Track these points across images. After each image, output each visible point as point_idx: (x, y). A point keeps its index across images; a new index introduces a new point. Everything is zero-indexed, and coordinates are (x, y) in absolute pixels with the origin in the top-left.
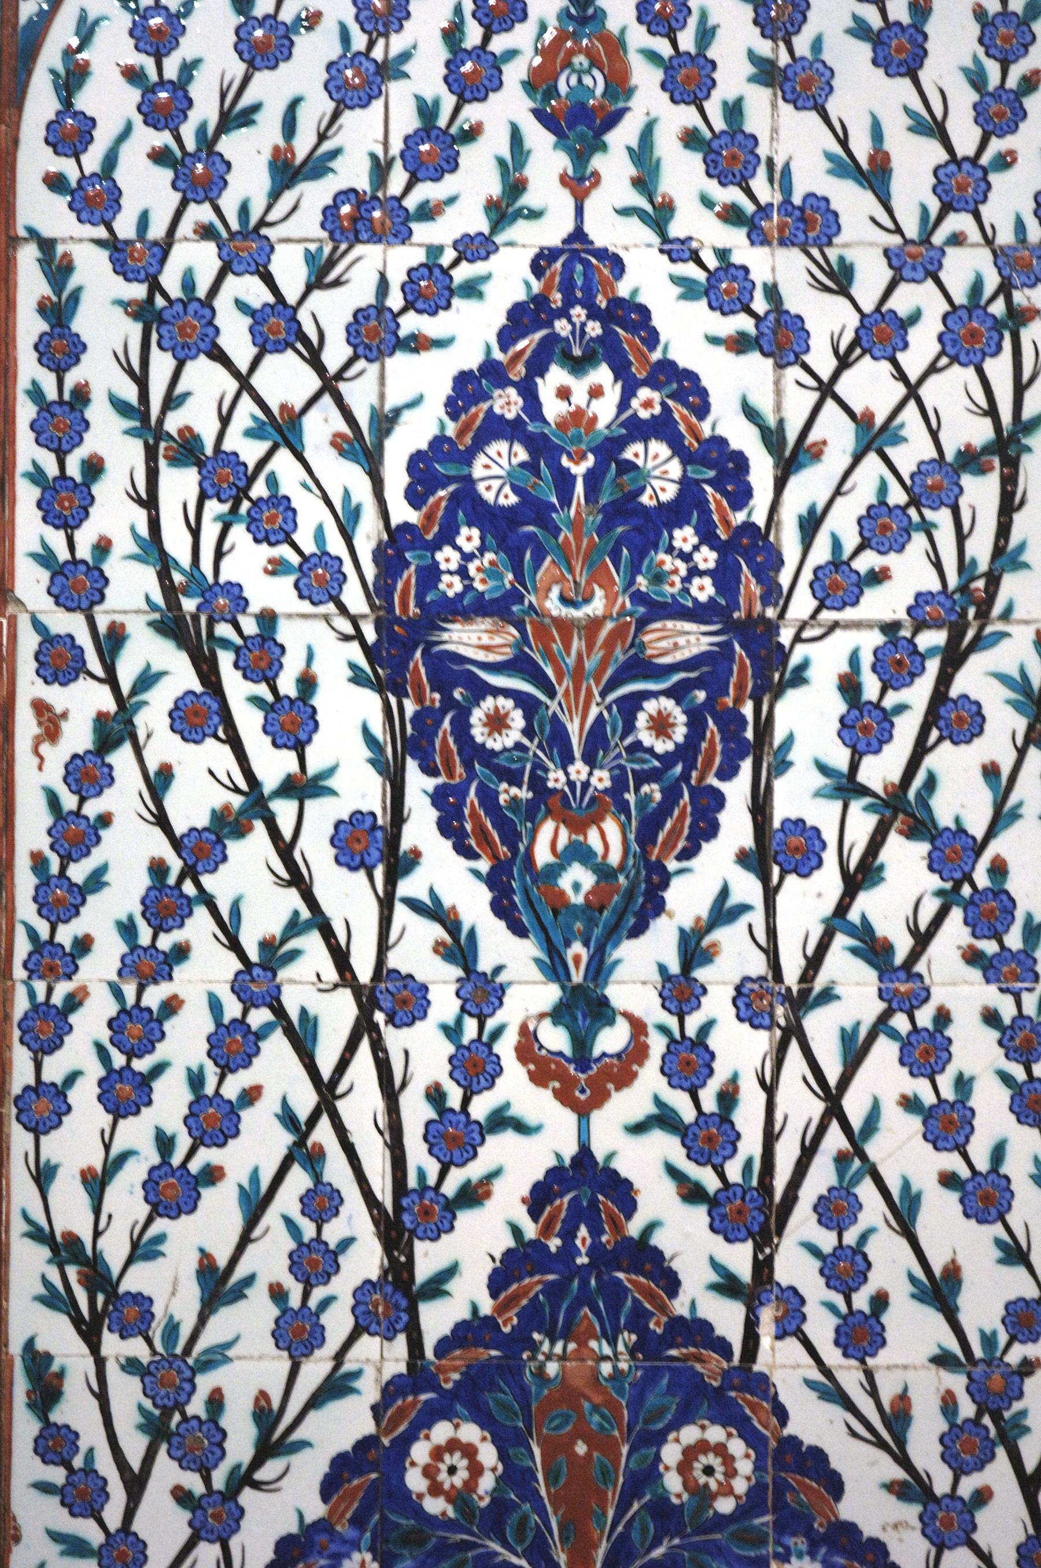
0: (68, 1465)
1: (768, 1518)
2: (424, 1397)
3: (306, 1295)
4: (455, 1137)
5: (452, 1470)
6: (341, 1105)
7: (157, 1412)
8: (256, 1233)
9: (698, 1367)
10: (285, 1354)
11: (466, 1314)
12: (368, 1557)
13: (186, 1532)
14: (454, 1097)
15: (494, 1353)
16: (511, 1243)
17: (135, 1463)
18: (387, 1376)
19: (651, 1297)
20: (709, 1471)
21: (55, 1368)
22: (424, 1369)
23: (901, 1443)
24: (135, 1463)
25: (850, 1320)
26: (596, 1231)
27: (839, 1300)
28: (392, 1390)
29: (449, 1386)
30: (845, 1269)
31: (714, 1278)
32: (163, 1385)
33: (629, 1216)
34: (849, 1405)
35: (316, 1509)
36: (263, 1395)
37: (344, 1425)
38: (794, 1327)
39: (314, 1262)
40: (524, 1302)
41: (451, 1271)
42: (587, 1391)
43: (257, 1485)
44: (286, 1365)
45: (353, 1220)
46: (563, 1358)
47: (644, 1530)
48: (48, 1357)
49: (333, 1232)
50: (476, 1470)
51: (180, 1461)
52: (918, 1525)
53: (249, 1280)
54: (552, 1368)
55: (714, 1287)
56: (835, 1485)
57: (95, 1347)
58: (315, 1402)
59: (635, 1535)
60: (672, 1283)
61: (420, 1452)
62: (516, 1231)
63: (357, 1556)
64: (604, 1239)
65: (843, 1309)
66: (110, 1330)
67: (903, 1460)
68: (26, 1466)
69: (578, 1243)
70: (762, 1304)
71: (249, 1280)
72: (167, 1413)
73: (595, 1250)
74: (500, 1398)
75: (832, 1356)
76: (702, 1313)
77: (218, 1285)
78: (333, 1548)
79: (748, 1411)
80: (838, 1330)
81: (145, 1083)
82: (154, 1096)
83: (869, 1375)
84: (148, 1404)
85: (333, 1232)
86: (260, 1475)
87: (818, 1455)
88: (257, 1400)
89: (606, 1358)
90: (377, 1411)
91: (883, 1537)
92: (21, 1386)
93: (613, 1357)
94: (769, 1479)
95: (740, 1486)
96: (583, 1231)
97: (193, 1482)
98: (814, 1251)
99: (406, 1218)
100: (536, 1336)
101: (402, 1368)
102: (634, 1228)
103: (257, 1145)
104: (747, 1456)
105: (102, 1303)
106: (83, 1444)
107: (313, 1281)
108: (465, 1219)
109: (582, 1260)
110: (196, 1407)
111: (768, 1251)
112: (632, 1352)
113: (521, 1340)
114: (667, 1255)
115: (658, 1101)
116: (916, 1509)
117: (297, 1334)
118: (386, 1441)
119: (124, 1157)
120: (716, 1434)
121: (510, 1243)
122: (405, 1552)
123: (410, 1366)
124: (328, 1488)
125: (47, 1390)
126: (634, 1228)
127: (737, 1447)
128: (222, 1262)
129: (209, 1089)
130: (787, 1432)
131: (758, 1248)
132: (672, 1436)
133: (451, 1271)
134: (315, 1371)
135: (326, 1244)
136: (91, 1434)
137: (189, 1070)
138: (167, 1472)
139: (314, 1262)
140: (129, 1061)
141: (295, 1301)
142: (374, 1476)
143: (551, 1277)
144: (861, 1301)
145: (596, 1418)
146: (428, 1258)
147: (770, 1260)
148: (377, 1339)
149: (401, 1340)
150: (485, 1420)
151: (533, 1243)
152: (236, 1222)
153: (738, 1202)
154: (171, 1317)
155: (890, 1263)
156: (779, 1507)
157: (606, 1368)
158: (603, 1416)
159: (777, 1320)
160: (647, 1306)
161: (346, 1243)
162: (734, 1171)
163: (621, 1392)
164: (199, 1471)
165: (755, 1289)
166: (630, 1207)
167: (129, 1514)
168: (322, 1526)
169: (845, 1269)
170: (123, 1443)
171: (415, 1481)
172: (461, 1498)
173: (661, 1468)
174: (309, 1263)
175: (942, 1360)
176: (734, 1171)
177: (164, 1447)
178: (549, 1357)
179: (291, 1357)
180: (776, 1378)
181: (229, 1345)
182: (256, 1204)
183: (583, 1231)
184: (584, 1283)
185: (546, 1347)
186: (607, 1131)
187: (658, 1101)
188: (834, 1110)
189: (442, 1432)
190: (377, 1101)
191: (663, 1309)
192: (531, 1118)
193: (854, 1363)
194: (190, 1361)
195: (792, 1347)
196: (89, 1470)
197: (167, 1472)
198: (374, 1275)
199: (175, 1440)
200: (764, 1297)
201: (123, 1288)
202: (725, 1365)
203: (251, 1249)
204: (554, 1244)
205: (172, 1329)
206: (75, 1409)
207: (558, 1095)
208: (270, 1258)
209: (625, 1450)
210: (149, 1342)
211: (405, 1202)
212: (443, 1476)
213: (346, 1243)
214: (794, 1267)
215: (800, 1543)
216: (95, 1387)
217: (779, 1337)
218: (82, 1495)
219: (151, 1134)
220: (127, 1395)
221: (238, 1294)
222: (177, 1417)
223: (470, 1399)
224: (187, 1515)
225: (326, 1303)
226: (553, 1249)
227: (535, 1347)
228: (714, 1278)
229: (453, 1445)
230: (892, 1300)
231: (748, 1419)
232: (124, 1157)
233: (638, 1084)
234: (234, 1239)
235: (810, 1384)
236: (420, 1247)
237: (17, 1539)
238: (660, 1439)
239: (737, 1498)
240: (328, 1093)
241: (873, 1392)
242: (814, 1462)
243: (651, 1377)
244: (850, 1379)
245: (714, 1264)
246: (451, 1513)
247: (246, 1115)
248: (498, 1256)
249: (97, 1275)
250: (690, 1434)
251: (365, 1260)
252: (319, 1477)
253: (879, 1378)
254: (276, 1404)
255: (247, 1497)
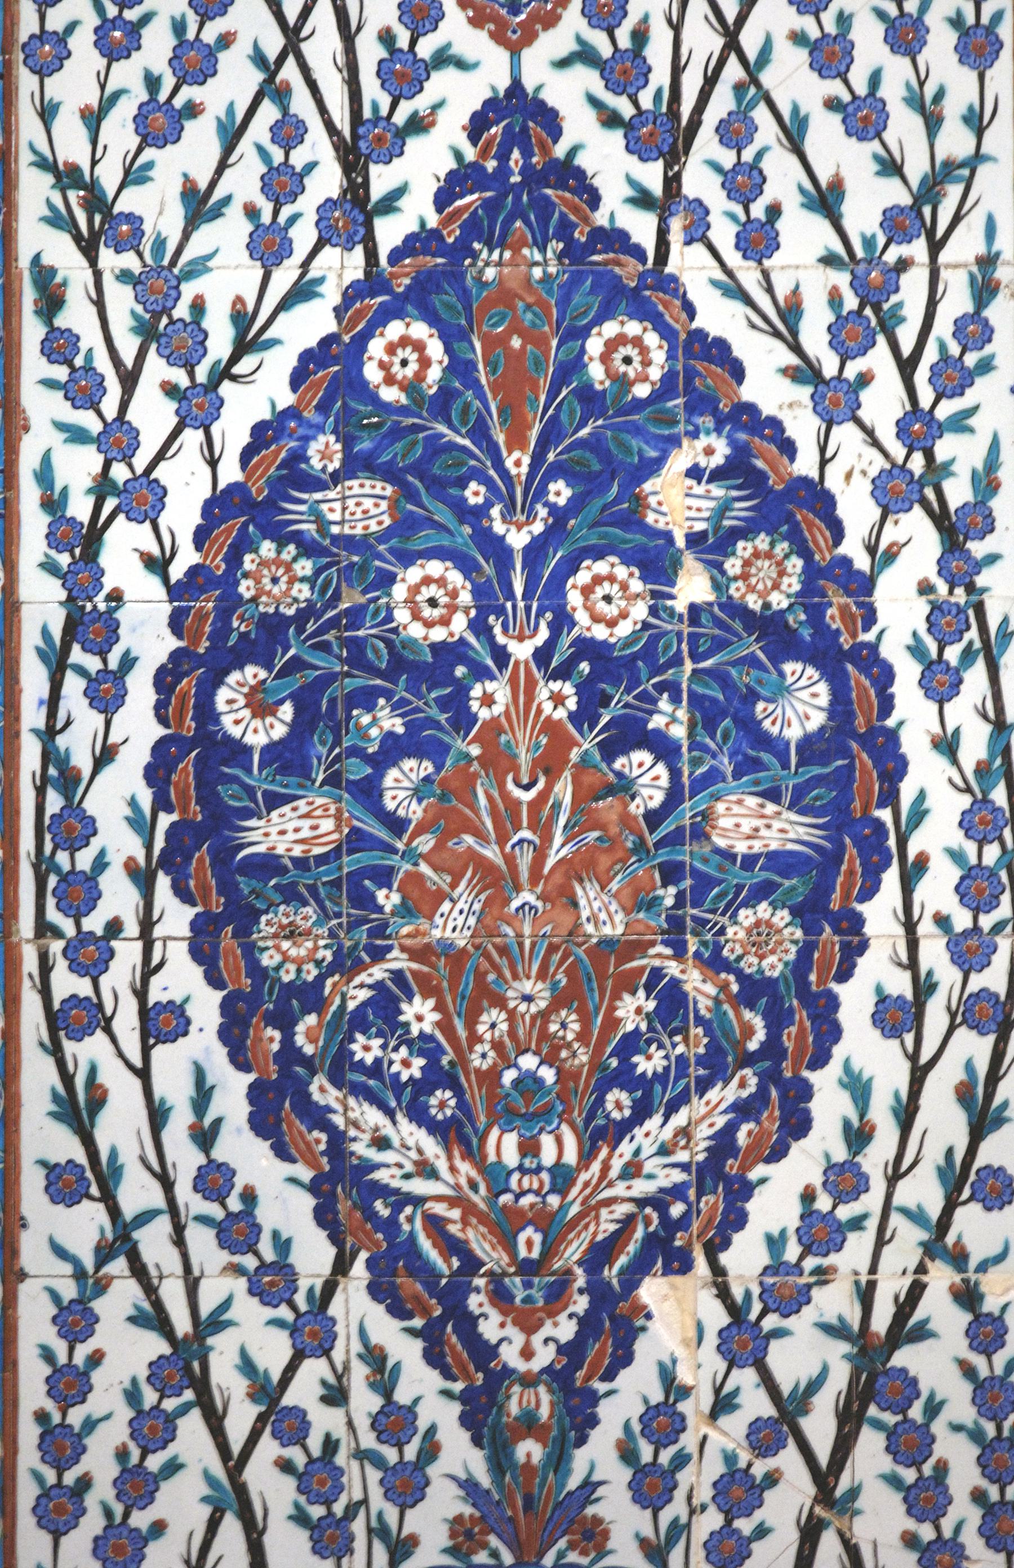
0: (70, 363)
1: (680, 401)
2: (380, 299)
3: (276, 213)
4: (405, 74)
5: (404, 363)
6: (304, 47)
7: (147, 316)
8: (232, 160)
9: (617, 270)
10: (259, 263)
11: (415, 228)
12: (332, 439)
13: (174, 420)
14: (403, 40)
15: (440, 260)
16: (453, 165)
17: (129, 361)
18: (346, 282)
19: (576, 210)
20: (627, 360)
21: (58, 279)
22: (379, 275)
23: (794, 333)
24: (129, 361)
25: (749, 227)
26: (527, 154)
27: (738, 210)
28: (352, 294)
29: (401, 289)
30: (744, 182)
31: (630, 192)
32: (153, 293)
33: (555, 141)
34: (748, 301)
35: (286, 399)
36: (239, 300)
37: (311, 324)
38: (700, 232)
39: (283, 184)
40: (466, 216)
41: (400, 191)
42: (520, 292)
43: (234, 378)
44: (260, 272)
45: (317, 148)
46: (499, 264)
47: (572, 413)
48: (53, 271)
49: (299, 158)
50: (425, 363)
51: (168, 358)
52: (811, 405)
53: (227, 200)
54: (490, 273)
55: (631, 201)
56: (738, 372)
57: (93, 261)
58: (284, 304)
59: (564, 417)
60: (594, 199)
61: (376, 347)
62: (458, 156)
63: (322, 439)
64: (535, 160)
65: (743, 218)
66: (106, 245)
67: (797, 348)
68: (33, 365)
69: (512, 163)
70: (671, 215)
71: (227, 200)
72: (156, 316)
73: (527, 170)
74: (445, 299)
75: (733, 258)
76: (621, 223)
77: (200, 205)
78: (301, 431)
79: (661, 308)
80: (738, 235)
81: (134, 30)
82: (143, 42)
83: (766, 274)
84: (139, 309)
85: (299, 158)
86: (236, 370)
87: (722, 345)
88: (234, 304)
89: (536, 264)
90: (338, 312)
91: (780, 415)
92: (29, 296)
93: (543, 263)
94: (679, 367)
95: (655, 373)
96: (516, 154)
97: (180, 377)
98: (717, 168)
99: (362, 145)
100: (476, 246)
101: (360, 275)
102: (560, 151)
103: (234, 82)
104: (661, 347)
105: (98, 223)
106: (84, 345)
107: (282, 200)
108: (413, 144)
109: (516, 179)
110: (182, 311)
111: (676, 168)
112: (560, 257)
113: (463, 249)
114: (589, 174)
115: (579, 40)
116: (809, 390)
117: (268, 246)
118: (346, 339)
119: (116, 95)
120: (633, 328)
121: (453, 165)
122: (364, 434)
123: (367, 273)
124: (296, 380)
125: (52, 301)
126: (560, 151)
127: (652, 339)
128: (203, 185)
129: (191, 35)
130: (695, 325)
131: (668, 166)
132: (595, 331)
133: (400, 191)
134: (284, 278)
135: (293, 168)
136: (91, 338)
137: (173, 18)
138: (157, 369)
139: (283, 184)
140: (121, 12)
141: (266, 218)
142: (336, 368)
143: (489, 194)
144: (758, 210)
145: (529, 316)
146: (381, 180)
147: (678, 177)
148: (338, 250)
149: (359, 251)
150: (432, 319)
151: (473, 165)
152: (214, 151)
153: (650, 126)
154: (159, 234)
155: (782, 179)
156: (689, 389)
157: (537, 272)
158: (535, 314)
159: (686, 228)
160: (572, 217)
161: (311, 167)
162: (646, 100)
163: (550, 292)
164: (184, 366)
165: (665, 201)
166: (556, 133)
167: (124, 406)
168: (292, 412)
169: (744, 182)
170: (119, 343)
171: (372, 373)
172: (412, 387)
173: (586, 358)
174: (278, 183)
175: (829, 260)
176: (646, 100)
177: (154, 346)
178: (487, 264)
179: (263, 266)
180: (685, 278)
181: (210, 257)
182: (231, 135)
183: (516, 154)
184: (518, 199)
185: (484, 255)
186: (537, 67)
187: (579, 40)
188: (732, 44)
189: (395, 330)
190: (336, 43)
191: (586, 220)
192: (470, 57)
193: (752, 264)
194: (176, 271)
195: (698, 250)
196: (89, 368)
197: (157, 369)
198: (335, 194)
199: (163, 340)
200: (673, 208)
201: (116, 210)
202: (641, 268)
203: (228, 173)
204: (491, 165)
205: (160, 244)
206: (77, 316)
207: (492, 35)
208: (244, 181)
209: (554, 343)
210: (140, 255)
211: (361, 131)
212: (396, 368)
213: (311, 167)
214: (699, 181)
215: (707, 421)
216: (94, 295)
217: (688, 243)
218: (83, 391)
219: (141, 74)
220: (121, 301)
221: (216, 213)
222: (165, 321)
223: (418, 299)
224: (175, 405)
225: (293, 219)
226: (490, 170)
227: (475, 255)
228: (630, 192)
229: (404, 341)
230: (785, 208)
231: (662, 315)
232: (116, 95)
233: (562, 24)
234: (213, 164)
235: (715, 283)
236: (374, 170)
237: (26, 429)
238: (584, 333)
239: (653, 384)
240: (293, 36)
241: (770, 290)
242: (720, 352)
243: (576, 280)
244: (749, 278)
245: (631, 181)
246: (404, 400)
247: (223, 57)
248: (442, 177)
249: (96, 201)
250: (610, 329)
251: (327, 181)
252: (289, 370)
253: (774, 277)
254: (250, 308)
255: (226, 388)
